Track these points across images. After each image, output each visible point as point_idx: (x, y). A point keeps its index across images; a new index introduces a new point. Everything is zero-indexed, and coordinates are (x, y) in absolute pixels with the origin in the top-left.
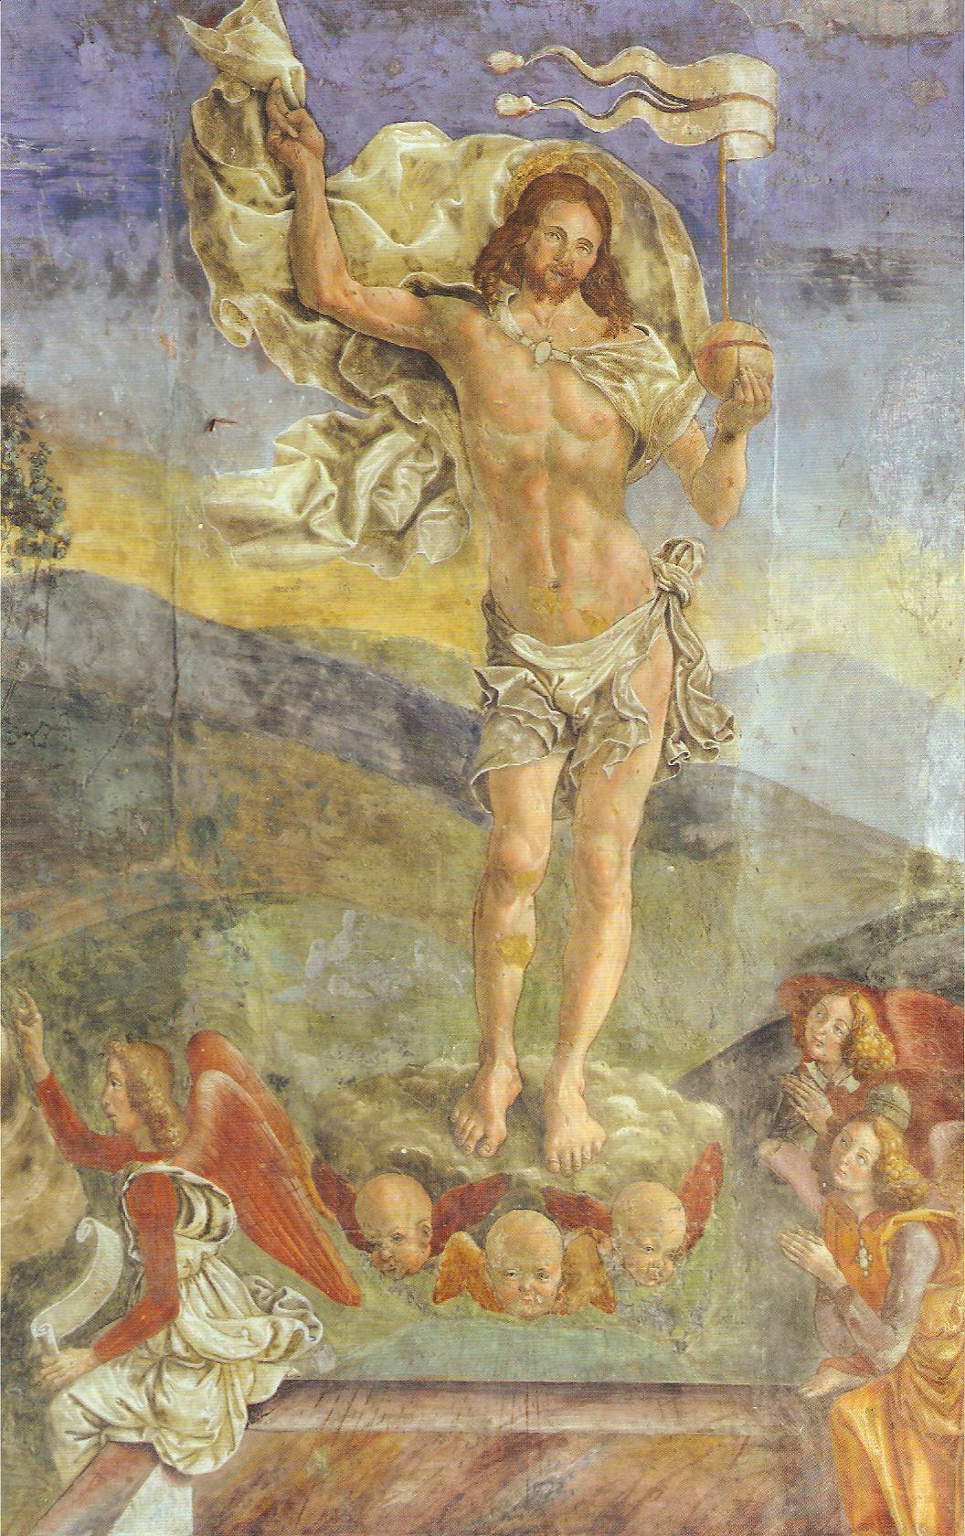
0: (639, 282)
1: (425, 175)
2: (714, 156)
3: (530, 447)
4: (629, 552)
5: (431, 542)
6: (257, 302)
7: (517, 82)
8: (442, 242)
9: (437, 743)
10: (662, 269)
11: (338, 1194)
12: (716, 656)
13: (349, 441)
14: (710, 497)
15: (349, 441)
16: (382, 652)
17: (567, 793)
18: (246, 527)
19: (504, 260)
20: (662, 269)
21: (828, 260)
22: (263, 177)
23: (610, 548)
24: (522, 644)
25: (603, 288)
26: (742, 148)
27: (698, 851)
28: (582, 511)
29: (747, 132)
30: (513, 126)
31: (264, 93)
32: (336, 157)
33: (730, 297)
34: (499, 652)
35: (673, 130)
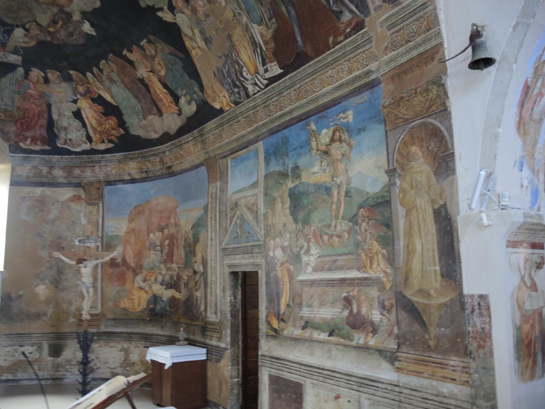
0: (343, 138)
1: (326, 134)
2: (348, 122)
3: (335, 158)
4: (343, 166)
5: (327, 171)
6: (315, 151)
7: (332, 122)
8: (328, 140)
9: (328, 190)
10: (345, 136)
11: (321, 237)
12: (350, 176)
13: (321, 162)
14: (349, 159)
15: (321, 162)
16: (324, 183)
17: (338, 193)
18: (314, 173)
19: (332, 140)
20: (345, 136)
21: (359, 129)
22: (314, 139)
23: (341, 166)
24: (335, 179)
25: (340, 140)
26: (350, 120)
27: (349, 196)
28: (339, 163)
29: (350, 119)
30: (332, 126)
31: (313, 131)
32: (319, 135)
33: (350, 136)
34: (333, 180)
35: (344, 121)
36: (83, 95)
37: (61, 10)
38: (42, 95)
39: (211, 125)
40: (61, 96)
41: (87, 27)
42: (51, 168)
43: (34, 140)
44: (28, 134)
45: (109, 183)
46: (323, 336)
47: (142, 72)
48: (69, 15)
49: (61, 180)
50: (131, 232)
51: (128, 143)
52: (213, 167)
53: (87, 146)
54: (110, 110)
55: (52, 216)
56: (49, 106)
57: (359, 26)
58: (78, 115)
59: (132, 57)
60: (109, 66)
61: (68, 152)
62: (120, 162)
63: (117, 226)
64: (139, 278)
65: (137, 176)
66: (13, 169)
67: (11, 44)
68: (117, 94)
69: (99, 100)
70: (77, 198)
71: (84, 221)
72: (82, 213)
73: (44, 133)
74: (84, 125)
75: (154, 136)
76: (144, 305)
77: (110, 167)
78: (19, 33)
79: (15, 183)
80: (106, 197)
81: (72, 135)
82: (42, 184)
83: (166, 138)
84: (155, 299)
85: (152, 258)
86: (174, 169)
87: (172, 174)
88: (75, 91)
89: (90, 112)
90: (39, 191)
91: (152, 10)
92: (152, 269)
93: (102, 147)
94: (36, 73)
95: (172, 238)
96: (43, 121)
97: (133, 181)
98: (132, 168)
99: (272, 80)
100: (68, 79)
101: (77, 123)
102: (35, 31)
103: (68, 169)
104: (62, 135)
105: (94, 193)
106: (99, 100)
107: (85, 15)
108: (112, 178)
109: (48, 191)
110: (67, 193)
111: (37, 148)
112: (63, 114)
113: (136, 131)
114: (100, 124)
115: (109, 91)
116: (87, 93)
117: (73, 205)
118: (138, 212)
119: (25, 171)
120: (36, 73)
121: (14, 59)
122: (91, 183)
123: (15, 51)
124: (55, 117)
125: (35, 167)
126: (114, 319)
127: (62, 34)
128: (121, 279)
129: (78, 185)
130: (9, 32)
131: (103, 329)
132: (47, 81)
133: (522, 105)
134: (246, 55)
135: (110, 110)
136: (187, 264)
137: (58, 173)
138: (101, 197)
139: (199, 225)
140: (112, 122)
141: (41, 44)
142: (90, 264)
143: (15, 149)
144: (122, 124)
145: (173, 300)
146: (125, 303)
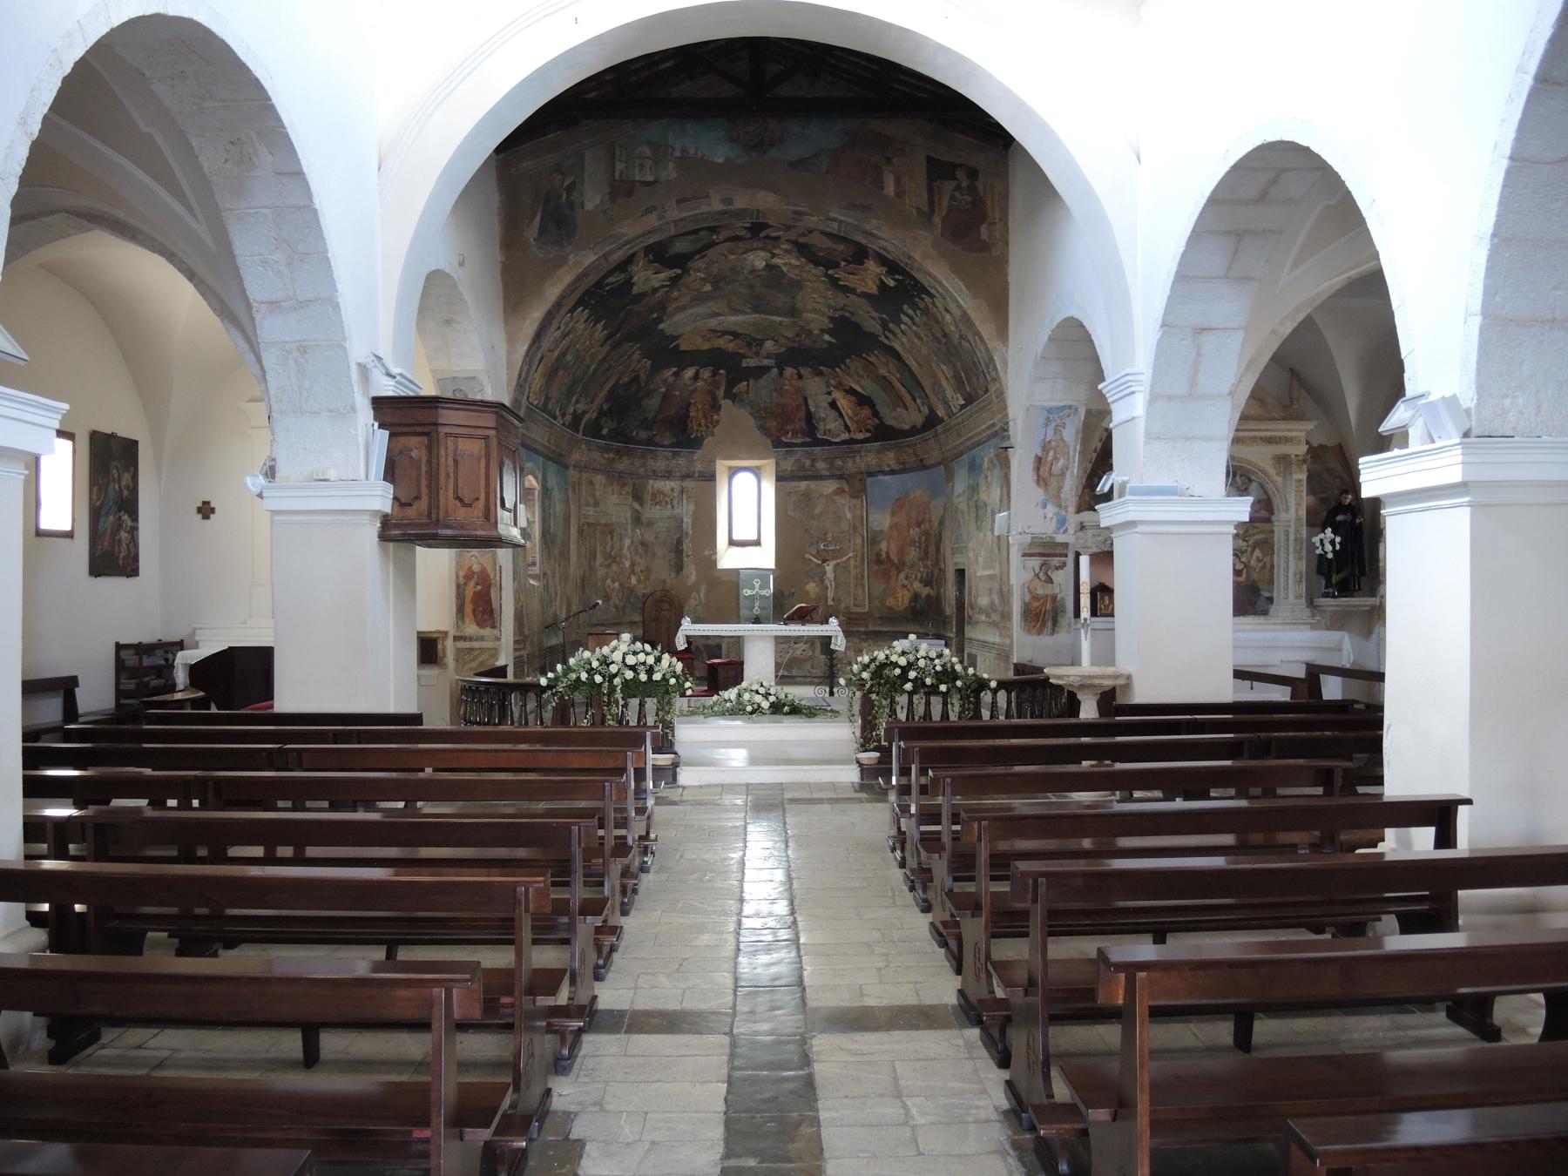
36: (836, 387)
37: (802, 328)
38: (798, 390)
39: (940, 428)
40: (816, 391)
41: (827, 337)
42: (813, 460)
43: (795, 433)
44: (789, 427)
45: (871, 474)
46: (983, 618)
47: (883, 371)
48: (811, 331)
49: (825, 473)
50: (894, 526)
51: (884, 434)
52: (947, 464)
53: (845, 436)
54: (863, 400)
55: (817, 511)
56: (805, 399)
57: (987, 391)
58: (833, 405)
59: (873, 359)
60: (854, 364)
61: (829, 443)
62: (879, 452)
63: (881, 520)
64: (902, 575)
65: (896, 467)
66: (777, 464)
67: (763, 353)
68: (865, 386)
69: (851, 392)
70: (840, 491)
71: (849, 516)
72: (847, 508)
73: (803, 424)
74: (841, 416)
75: (906, 427)
76: (906, 603)
77: (870, 457)
78: (769, 345)
79: (780, 478)
80: (869, 489)
81: (830, 425)
82: (806, 478)
83: (914, 431)
84: (916, 597)
85: (913, 554)
86: (927, 462)
87: (925, 468)
88: (828, 385)
89: (844, 403)
90: (803, 485)
91: (873, 336)
92: (913, 566)
93: (860, 436)
94: (789, 371)
95: (927, 533)
96: (802, 414)
97: (892, 472)
98: (890, 459)
99: (963, 407)
100: (821, 374)
101: (833, 413)
102: (783, 341)
103: (831, 461)
104: (822, 426)
105: (857, 484)
106: (851, 392)
107: (823, 331)
108: (872, 469)
109: (813, 485)
110: (830, 487)
111: (799, 441)
112: (819, 404)
113: (889, 422)
114: (856, 414)
115: (858, 383)
116: (839, 386)
117: (838, 499)
118: (899, 505)
119: (788, 465)
120: (789, 371)
121: (766, 362)
122: (852, 475)
123: (768, 357)
124: (812, 409)
125: (798, 460)
126: (881, 618)
127: (807, 342)
128: (886, 576)
129: (840, 477)
130: (761, 343)
131: (871, 628)
132: (800, 377)
133: (1038, 469)
134: (944, 383)
135: (863, 400)
136: (937, 563)
137: (821, 465)
138: (864, 490)
139: (941, 523)
140: (866, 412)
141: (790, 349)
142: (832, 563)
143: (777, 444)
144: (876, 414)
145: (929, 596)
146: (890, 602)
